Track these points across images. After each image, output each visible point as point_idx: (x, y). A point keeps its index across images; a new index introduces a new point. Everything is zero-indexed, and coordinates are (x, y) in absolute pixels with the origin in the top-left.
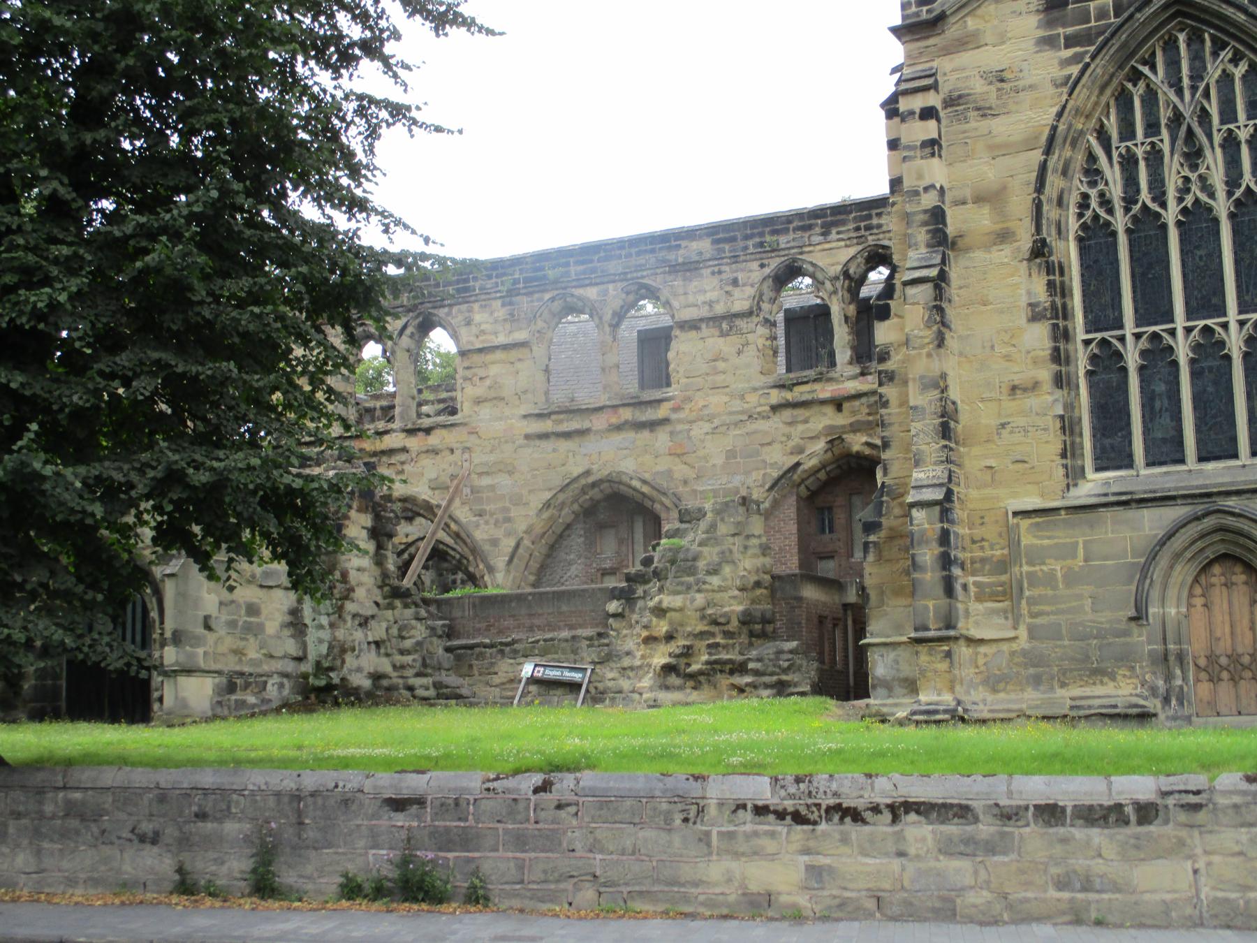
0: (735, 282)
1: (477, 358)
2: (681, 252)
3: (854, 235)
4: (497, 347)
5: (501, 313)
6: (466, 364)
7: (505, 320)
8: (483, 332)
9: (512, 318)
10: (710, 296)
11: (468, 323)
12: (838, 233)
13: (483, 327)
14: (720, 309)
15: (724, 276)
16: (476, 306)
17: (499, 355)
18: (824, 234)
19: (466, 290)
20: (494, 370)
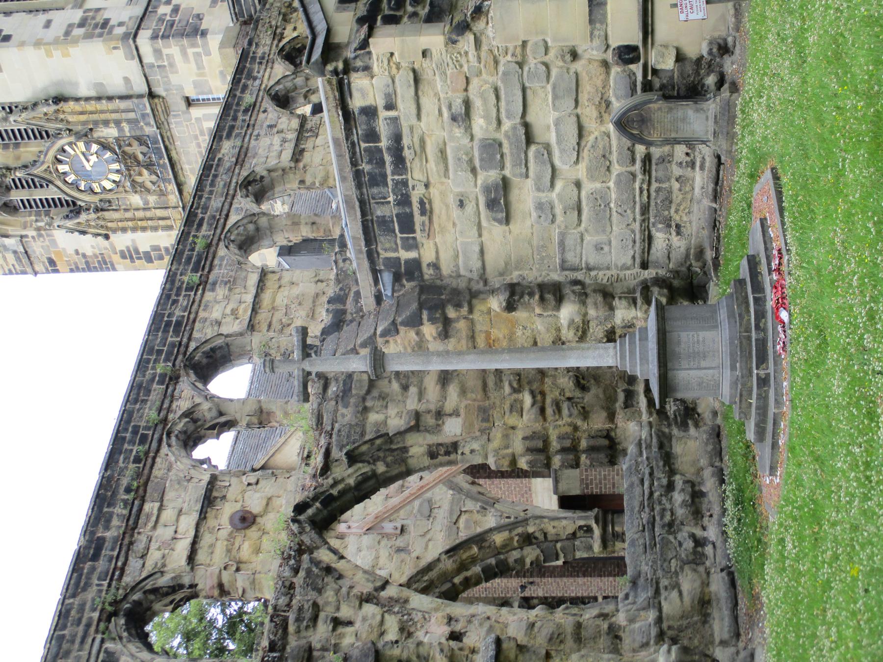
0: (271, 127)
1: (263, 316)
2: (226, 158)
3: (263, 67)
4: (257, 296)
5: (221, 291)
6: (264, 327)
7: (230, 290)
8: (234, 312)
9: (231, 284)
10: (277, 140)
11: (219, 323)
12: (258, 72)
13: (228, 311)
14: (292, 136)
15: (262, 133)
16: (202, 314)
17: (266, 297)
18: (255, 79)
19: (179, 324)
20: (281, 299)
